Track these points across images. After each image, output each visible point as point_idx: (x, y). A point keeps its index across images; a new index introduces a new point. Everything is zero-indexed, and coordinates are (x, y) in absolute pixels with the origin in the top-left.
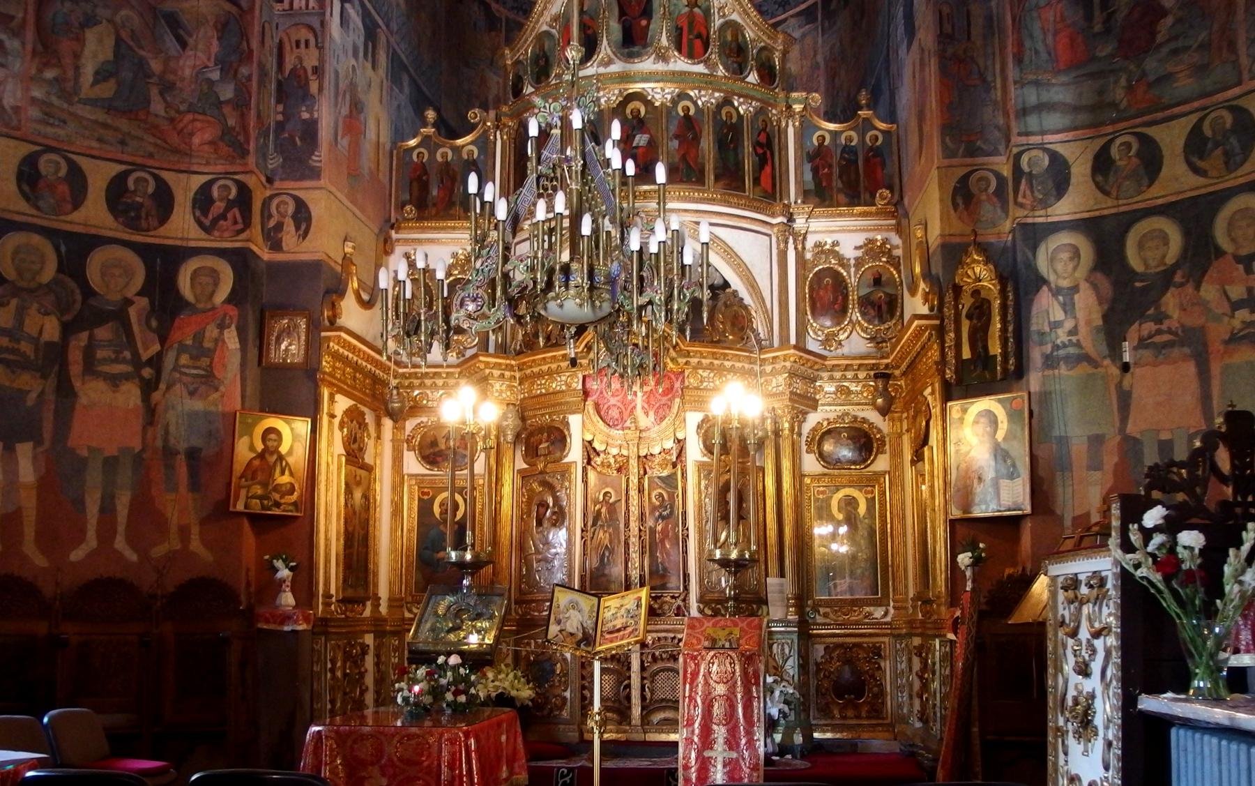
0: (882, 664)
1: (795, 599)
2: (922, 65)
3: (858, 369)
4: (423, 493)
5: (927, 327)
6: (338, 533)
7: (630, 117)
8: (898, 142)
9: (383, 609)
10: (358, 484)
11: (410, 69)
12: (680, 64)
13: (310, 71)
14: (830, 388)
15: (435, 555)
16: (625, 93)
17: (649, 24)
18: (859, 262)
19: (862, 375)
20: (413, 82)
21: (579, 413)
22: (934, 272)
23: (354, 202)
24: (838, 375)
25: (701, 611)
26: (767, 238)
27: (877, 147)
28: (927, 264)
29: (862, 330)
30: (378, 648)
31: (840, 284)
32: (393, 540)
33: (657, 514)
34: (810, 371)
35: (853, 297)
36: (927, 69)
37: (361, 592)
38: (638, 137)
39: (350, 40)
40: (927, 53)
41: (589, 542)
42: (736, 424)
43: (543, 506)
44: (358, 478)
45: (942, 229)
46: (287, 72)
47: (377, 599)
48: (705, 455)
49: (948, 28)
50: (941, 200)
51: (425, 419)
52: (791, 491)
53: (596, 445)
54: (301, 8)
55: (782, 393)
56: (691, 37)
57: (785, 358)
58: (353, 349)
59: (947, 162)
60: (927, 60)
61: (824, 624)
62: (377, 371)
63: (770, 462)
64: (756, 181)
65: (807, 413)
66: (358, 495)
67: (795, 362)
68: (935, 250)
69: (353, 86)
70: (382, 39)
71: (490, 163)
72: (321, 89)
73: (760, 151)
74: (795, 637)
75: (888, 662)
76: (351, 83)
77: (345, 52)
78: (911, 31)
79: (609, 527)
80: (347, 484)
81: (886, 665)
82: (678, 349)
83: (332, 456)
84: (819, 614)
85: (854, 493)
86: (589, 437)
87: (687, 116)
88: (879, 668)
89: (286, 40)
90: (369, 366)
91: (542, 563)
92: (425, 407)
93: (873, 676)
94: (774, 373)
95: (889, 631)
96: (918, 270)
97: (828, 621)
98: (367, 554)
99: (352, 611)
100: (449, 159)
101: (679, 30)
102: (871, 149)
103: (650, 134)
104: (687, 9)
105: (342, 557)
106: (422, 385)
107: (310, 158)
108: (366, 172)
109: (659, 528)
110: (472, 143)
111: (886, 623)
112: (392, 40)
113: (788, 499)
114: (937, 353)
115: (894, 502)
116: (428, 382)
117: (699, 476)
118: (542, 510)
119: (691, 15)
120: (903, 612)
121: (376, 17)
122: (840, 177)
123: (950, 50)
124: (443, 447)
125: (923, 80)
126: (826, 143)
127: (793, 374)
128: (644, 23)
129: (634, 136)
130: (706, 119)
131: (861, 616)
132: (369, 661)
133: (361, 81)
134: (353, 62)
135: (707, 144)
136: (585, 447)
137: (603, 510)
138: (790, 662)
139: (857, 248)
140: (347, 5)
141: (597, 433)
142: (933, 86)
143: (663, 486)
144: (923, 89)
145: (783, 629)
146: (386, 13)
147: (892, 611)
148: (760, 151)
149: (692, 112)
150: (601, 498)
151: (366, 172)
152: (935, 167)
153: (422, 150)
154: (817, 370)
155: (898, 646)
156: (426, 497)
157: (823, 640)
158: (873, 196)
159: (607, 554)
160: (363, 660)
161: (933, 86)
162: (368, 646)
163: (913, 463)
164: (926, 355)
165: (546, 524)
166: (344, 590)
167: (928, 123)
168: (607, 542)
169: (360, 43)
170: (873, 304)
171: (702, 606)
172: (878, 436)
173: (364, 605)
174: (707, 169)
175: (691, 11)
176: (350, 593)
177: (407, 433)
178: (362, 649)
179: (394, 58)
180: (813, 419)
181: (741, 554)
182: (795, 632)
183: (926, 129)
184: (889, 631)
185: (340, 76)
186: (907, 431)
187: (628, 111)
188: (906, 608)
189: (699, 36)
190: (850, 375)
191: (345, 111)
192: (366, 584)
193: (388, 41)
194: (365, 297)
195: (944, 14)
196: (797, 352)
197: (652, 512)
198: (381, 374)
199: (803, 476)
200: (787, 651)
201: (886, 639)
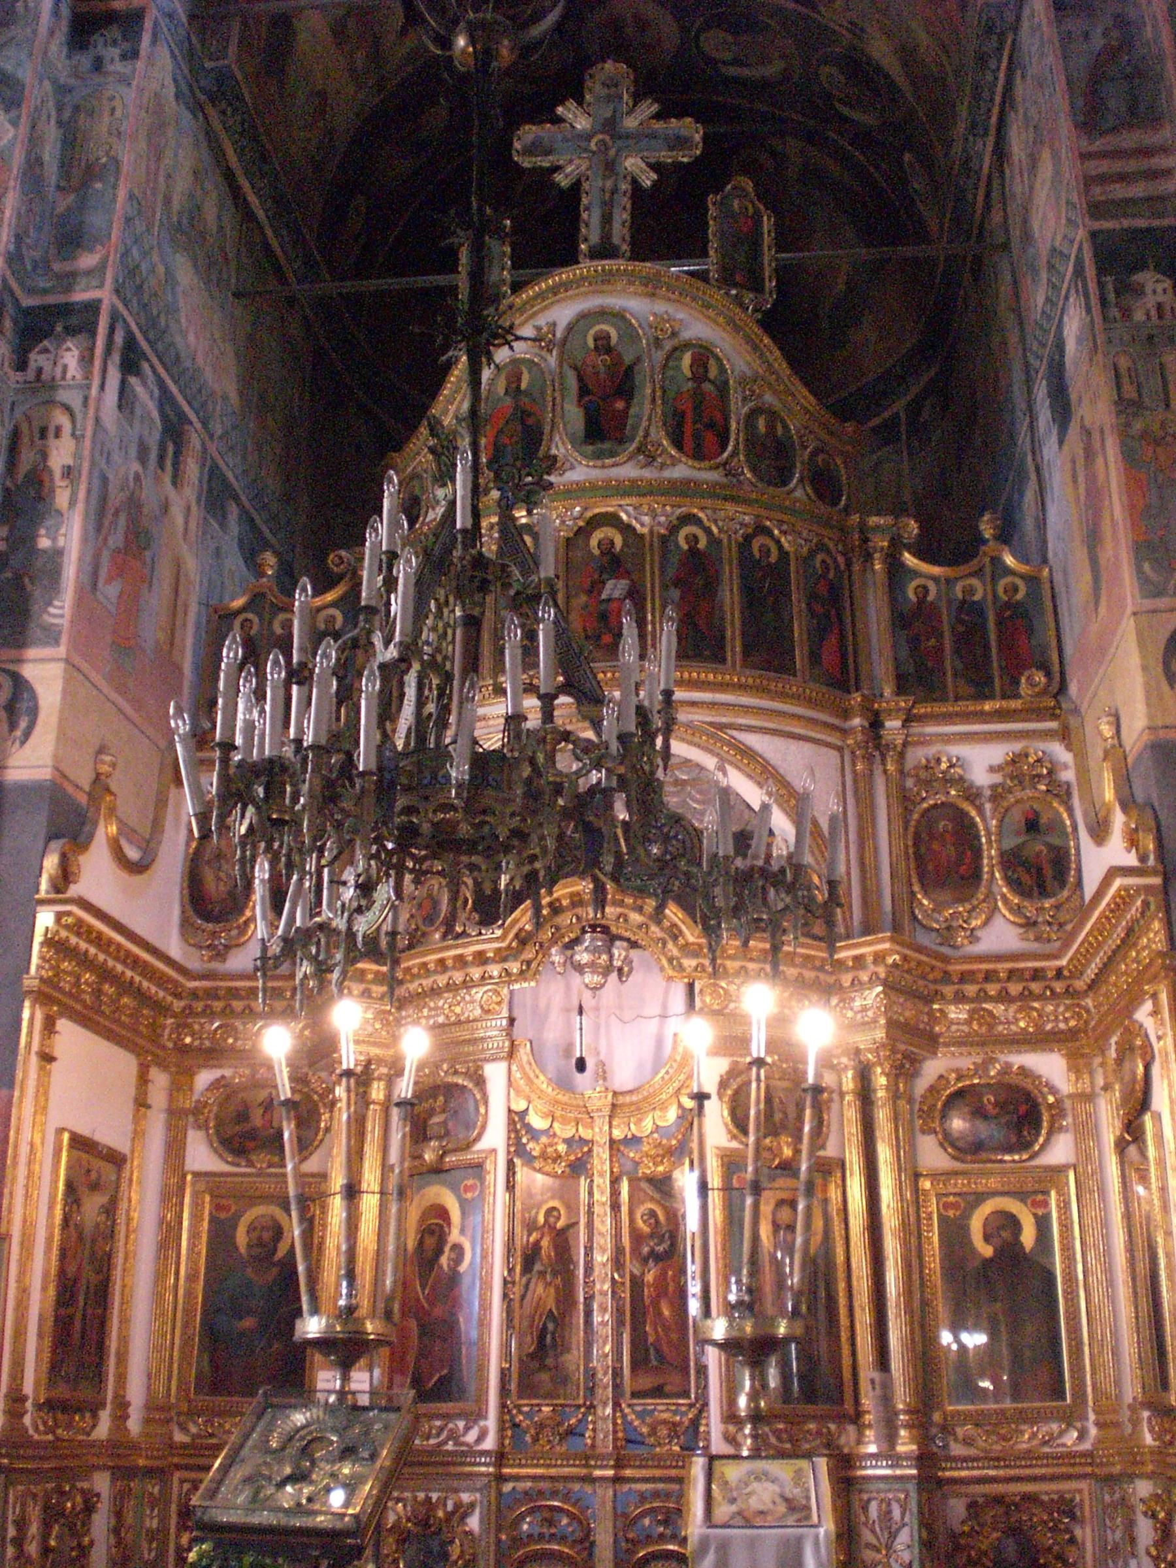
0: (1078, 1532)
2: (1089, 455)
3: (1009, 979)
5: (1138, 890)
6: (46, 1274)
7: (596, 552)
8: (1053, 597)
9: (134, 1425)
10: (95, 1187)
11: (243, 498)
12: (682, 470)
13: (57, 474)
14: (957, 1013)
18: (997, 793)
19: (1015, 988)
20: (244, 514)
22: (1140, 797)
23: (122, 690)
24: (971, 989)
26: (835, 753)
27: (1018, 603)
28: (1124, 781)
29: (1010, 910)
30: (120, 1498)
31: (965, 833)
32: (158, 1297)
33: (646, 1250)
34: (921, 983)
35: (990, 854)
36: (1100, 460)
37: (85, 1392)
38: (610, 584)
39: (134, 433)
40: (1096, 436)
41: (517, 1305)
44: (94, 1175)
45: (1151, 717)
46: (20, 477)
47: (122, 1406)
49: (1129, 391)
50: (1145, 668)
51: (228, 1072)
57: (879, 958)
58: (98, 940)
59: (1148, 603)
60: (1097, 445)
61: (965, 1459)
62: (145, 984)
64: (814, 657)
65: (920, 1062)
66: (92, 1205)
68: (1140, 755)
69: (134, 505)
70: (195, 440)
72: (72, 503)
74: (911, 1487)
75: (1088, 1530)
76: (131, 499)
77: (123, 447)
78: (1063, 411)
79: (555, 1274)
80: (70, 1187)
81: (1085, 1534)
82: (681, 941)
83: (43, 1132)
84: (956, 1440)
85: (1013, 1206)
86: (519, 1105)
87: (693, 551)
88: (1072, 1541)
89: (25, 428)
90: (129, 973)
92: (232, 1048)
93: (1060, 1558)
94: (856, 984)
95: (1089, 1470)
96: (1109, 795)
97: (972, 1452)
98: (103, 1323)
99: (69, 1426)
102: (1008, 605)
104: (690, 384)
105: (50, 1322)
106: (227, 1012)
107: (45, 611)
108: (149, 646)
109: (649, 1277)
110: (334, 604)
111: (1084, 1454)
112: (212, 448)
114: (1162, 936)
115: (1087, 1221)
116: (238, 1005)
119: (697, 393)
120: (1113, 1432)
121: (186, 408)
122: (957, 651)
123: (1138, 425)
125: (1091, 479)
126: (930, 598)
128: (620, 405)
129: (604, 583)
130: (725, 555)
131: (1035, 1442)
132: (101, 1523)
133: (149, 495)
134: (136, 467)
135: (730, 596)
136: (511, 1123)
137: (545, 1243)
138: (904, 1537)
139: (992, 769)
140: (133, 380)
141: (533, 1096)
142: (1114, 485)
143: (657, 1196)
144: (1094, 497)
145: (888, 1472)
146: (204, 404)
147: (1093, 1431)
149: (702, 544)
150: (541, 1219)
151: (149, 646)
152: (1129, 610)
153: (250, 616)
154: (935, 981)
155: (1107, 1498)
157: (963, 1489)
158: (1017, 683)
159: (551, 1326)
160: (87, 1523)
161: (1114, 485)
162: (98, 1495)
163: (1121, 1147)
164: (1135, 944)
166: (52, 1383)
167: (1109, 545)
168: (551, 1304)
169: (154, 438)
170: (1025, 864)
172: (1051, 1099)
173: (95, 1416)
174: (729, 633)
176: (62, 1391)
177: (195, 1098)
178: (86, 1501)
179: (214, 474)
180: (933, 1068)
182: (912, 1477)
183: (1106, 554)
184: (1089, 1470)
185: (111, 487)
186: (1107, 1087)
187: (594, 542)
188: (1117, 1425)
190: (992, 989)
191: (117, 539)
192: (99, 1378)
193: (205, 449)
194: (133, 854)
195: (1123, 371)
198: (153, 989)
199: (917, 1176)
200: (896, 1513)
201: (1083, 1485)
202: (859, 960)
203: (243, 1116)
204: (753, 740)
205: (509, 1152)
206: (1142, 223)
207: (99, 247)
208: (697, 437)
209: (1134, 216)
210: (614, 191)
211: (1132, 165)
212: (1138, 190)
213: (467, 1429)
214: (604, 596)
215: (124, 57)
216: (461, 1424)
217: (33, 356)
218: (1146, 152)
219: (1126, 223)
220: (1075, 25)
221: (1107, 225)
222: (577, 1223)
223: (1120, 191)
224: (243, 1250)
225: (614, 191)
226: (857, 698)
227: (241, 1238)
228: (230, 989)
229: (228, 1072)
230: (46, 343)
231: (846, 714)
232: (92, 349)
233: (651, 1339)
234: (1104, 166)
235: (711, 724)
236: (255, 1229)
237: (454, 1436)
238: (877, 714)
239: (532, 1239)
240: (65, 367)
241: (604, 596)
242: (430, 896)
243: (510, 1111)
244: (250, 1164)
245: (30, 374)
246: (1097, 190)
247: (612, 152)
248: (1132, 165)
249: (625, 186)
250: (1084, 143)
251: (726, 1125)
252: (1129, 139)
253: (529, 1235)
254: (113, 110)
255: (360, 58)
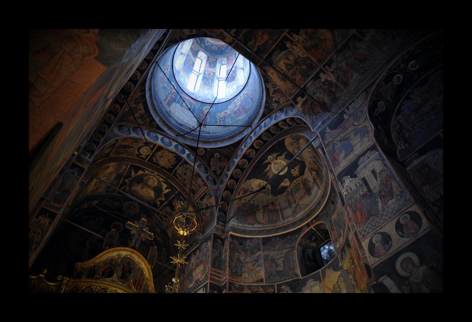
16: (117, 291)
17: (129, 276)
54: (42, 223)
56: (138, 284)
101: (136, 281)
104: (139, 276)
110: (55, 286)
175: (140, 277)
189: (140, 284)
206: (216, 284)
207: (61, 204)
208: (137, 286)
209: (216, 282)
210: (139, 239)
211: (217, 274)
212: (217, 279)
215: (78, 175)
217: (40, 217)
218: (219, 273)
219: (214, 283)
220: (215, 251)
221: (212, 282)
223: (215, 278)
225: (139, 239)
230: (43, 216)
232: (52, 222)
234: (214, 273)
240: (45, 222)
245: (38, 220)
246: (212, 276)
247: (140, 232)
248: (217, 274)
249: (140, 239)
250: (212, 268)
252: (218, 271)
254: (73, 183)
255: (95, 188)
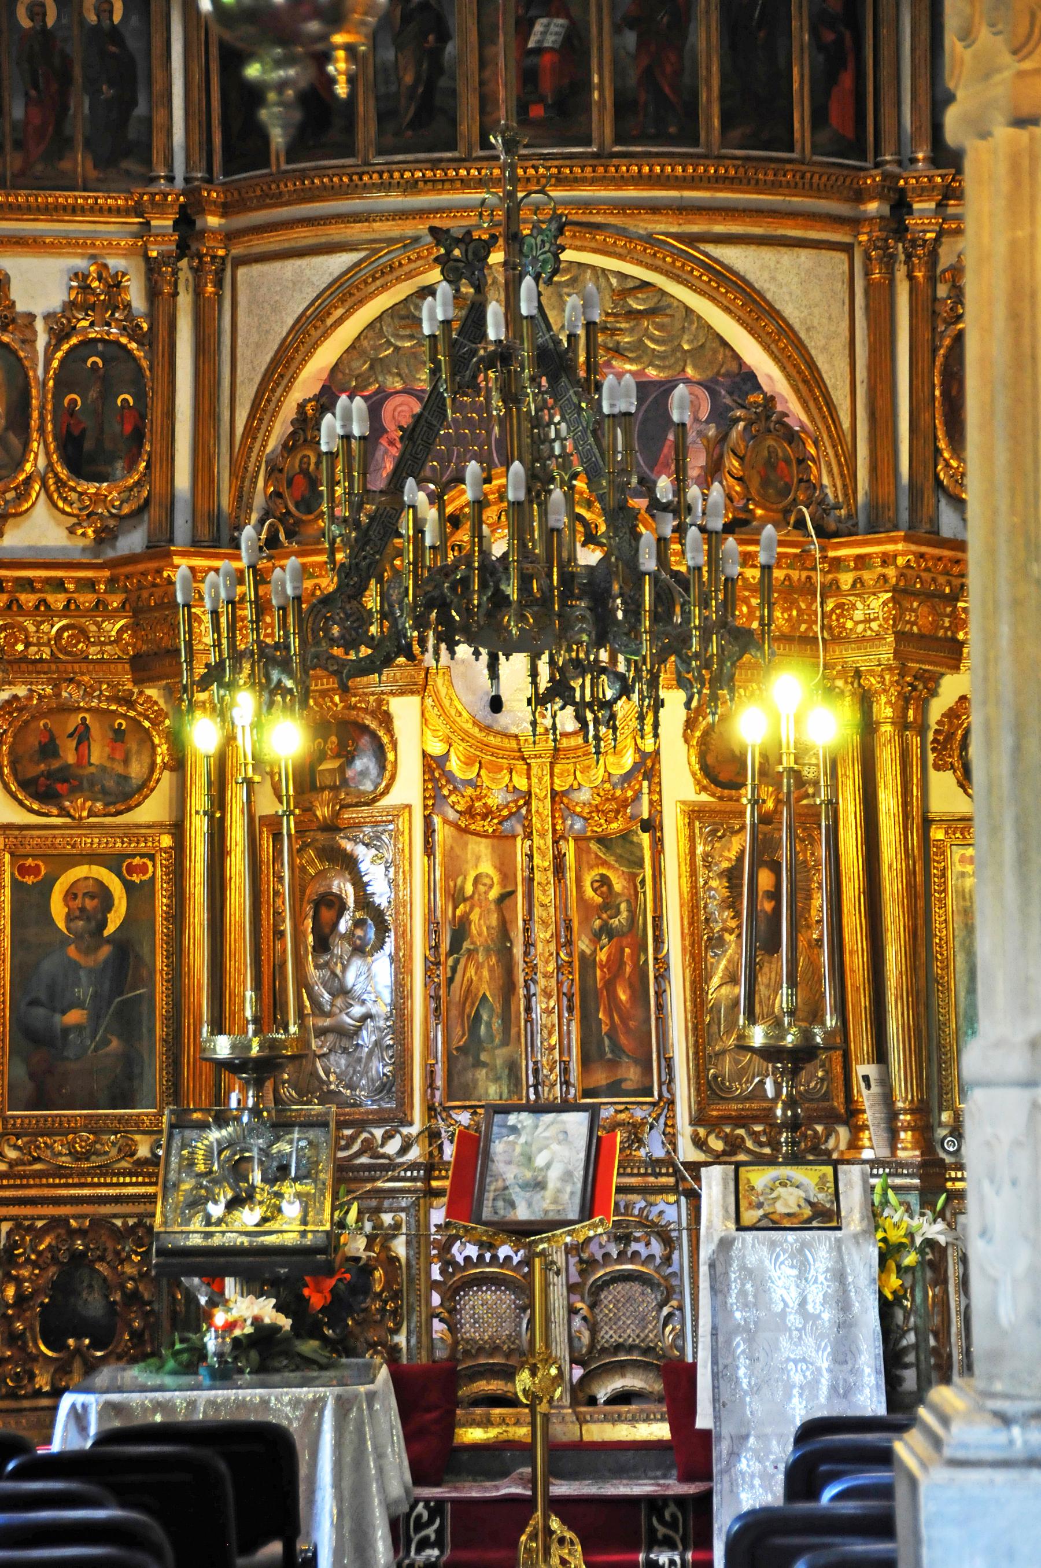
1: (912, 1111)
4: (23, 870)
15: (57, 1017)
21: (412, 692)
25: (699, 1143)
26: (843, 257)
42: (788, 762)
43: (330, 905)
48: (704, 789)
52: (899, 865)
53: (454, 766)
55: (879, 637)
57: (887, 560)
63: (850, 797)
64: (819, 118)
67: (908, 566)
71: (157, 41)
73: (829, 37)
86: (436, 748)
91: (331, 1037)
100: (50, 21)
103: (568, 16)
109: (602, 956)
113: (892, 885)
116: (28, 599)
117: (692, 839)
118: (327, 914)
124: (71, 758)
127: (901, 594)
129: (531, 24)
148: (829, 37)
156: (29, 880)
165: (341, 948)
171: (702, 1132)
174: (704, 97)
181: (807, 1035)
196: (913, 548)
197: (585, 920)
199: (927, 822)
202: (862, 561)
203: (49, 749)
204: (731, 255)
205: (426, 807)
213: (388, 1137)
214: (531, 44)
216: (378, 1133)
222: (513, 893)
224: (61, 924)
226: (873, 179)
227: (58, 909)
228: (17, 580)
229: (21, 691)
231: (859, 196)
233: (605, 1028)
235: (677, 237)
236: (75, 896)
237: (368, 1147)
238: (902, 191)
239: (458, 912)
241: (531, 44)
242: (304, 472)
243: (425, 754)
244: (64, 813)
251: (694, 774)
253: (455, 908)
